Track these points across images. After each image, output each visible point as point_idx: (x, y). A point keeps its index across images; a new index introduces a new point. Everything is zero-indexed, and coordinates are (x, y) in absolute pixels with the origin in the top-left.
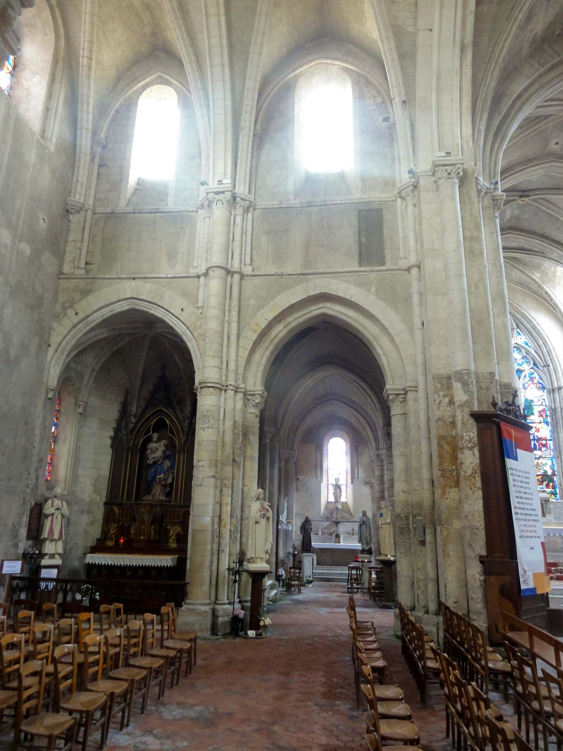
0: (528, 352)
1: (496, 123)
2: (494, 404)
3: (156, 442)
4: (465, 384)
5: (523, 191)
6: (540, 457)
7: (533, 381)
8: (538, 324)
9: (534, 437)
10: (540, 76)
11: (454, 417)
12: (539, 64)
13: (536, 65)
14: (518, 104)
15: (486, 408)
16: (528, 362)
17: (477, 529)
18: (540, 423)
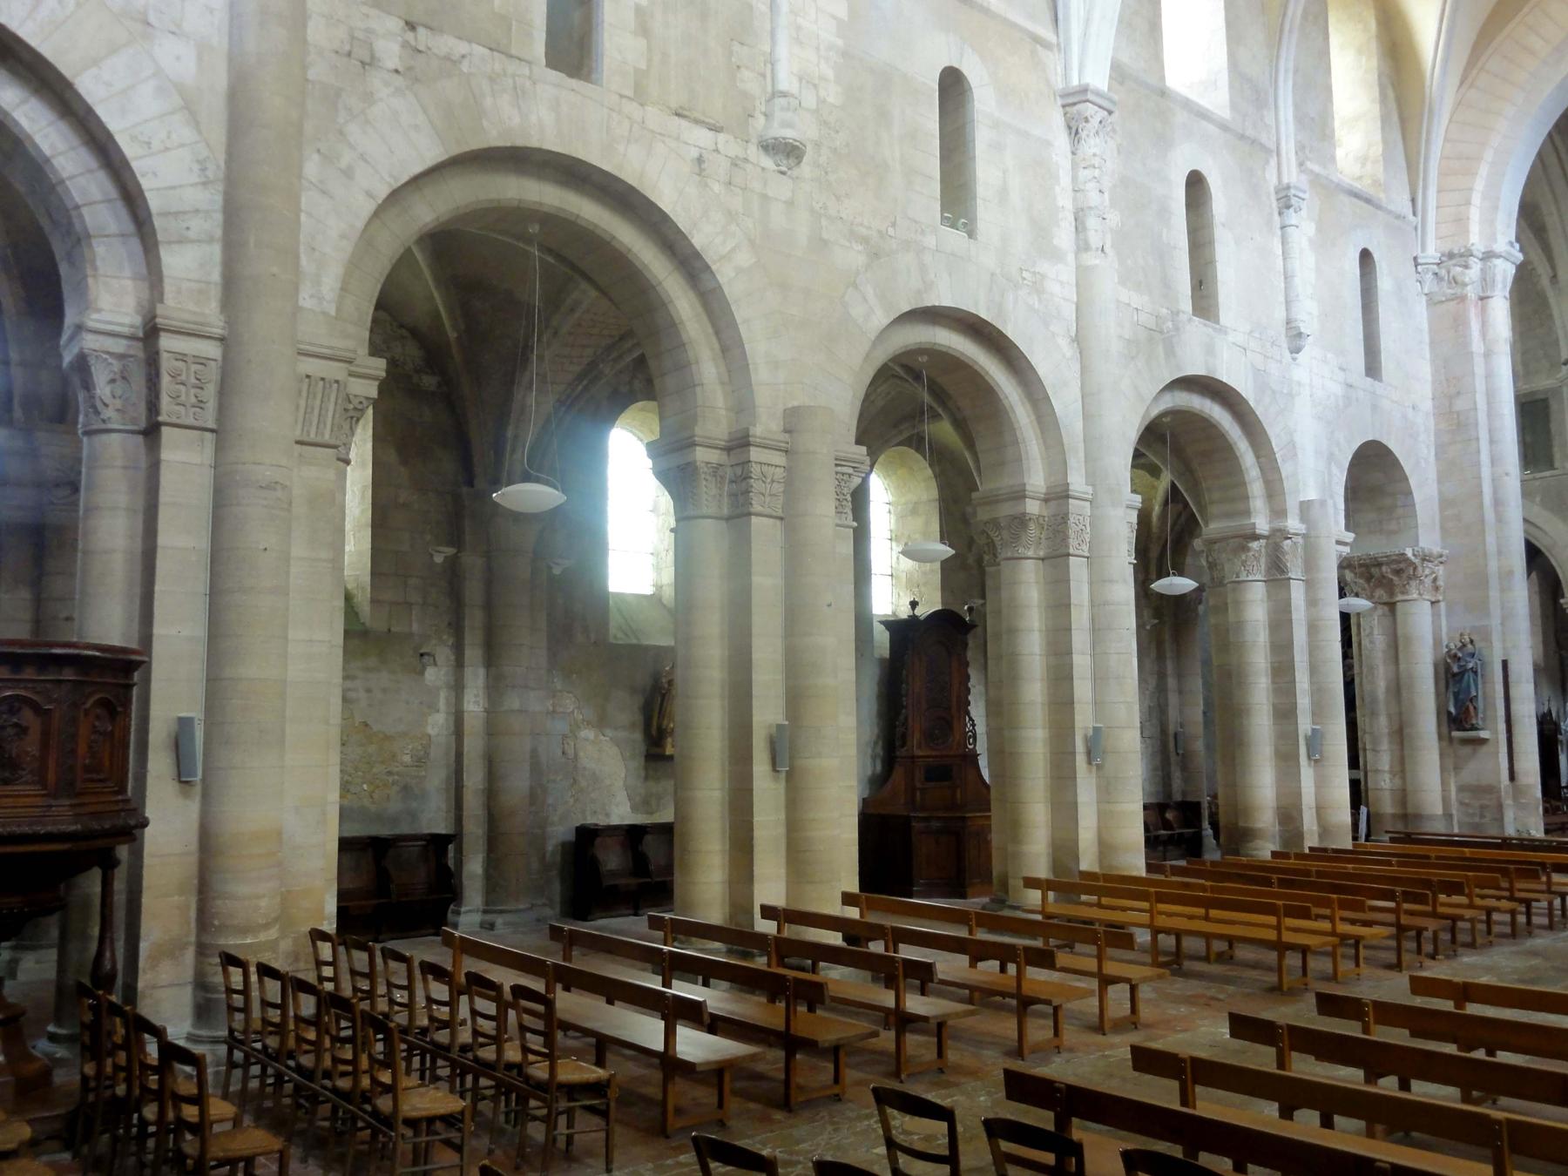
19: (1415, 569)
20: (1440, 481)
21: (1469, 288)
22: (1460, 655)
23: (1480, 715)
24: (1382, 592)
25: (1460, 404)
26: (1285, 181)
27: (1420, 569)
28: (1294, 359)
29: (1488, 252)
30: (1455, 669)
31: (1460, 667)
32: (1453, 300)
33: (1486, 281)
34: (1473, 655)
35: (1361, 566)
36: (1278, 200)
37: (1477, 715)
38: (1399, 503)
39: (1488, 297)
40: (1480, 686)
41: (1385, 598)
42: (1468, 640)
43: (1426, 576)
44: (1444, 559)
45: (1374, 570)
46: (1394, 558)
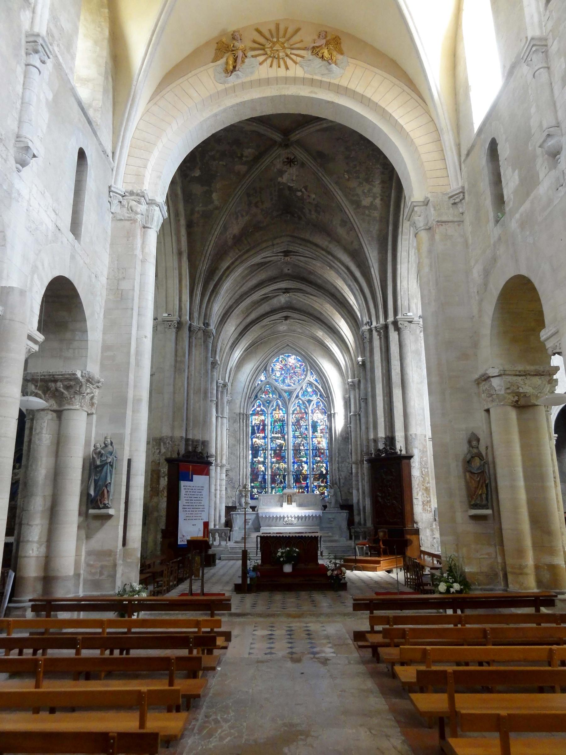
0: (316, 387)
1: (211, 287)
2: (178, 454)
3: (18, 469)
4: (165, 444)
5: (286, 289)
6: (319, 462)
7: (318, 408)
8: (323, 367)
9: (316, 447)
10: (240, 256)
11: (160, 460)
12: (239, 250)
13: (237, 251)
14: (228, 272)
15: (175, 456)
16: (317, 394)
17: (162, 516)
18: (321, 437)
19: (81, 387)
20: (104, 333)
21: (139, 216)
22: (103, 452)
23: (111, 498)
24: (54, 402)
25: (124, 285)
26: (36, 30)
27: (84, 387)
28: (19, 171)
29: (152, 200)
30: (98, 463)
31: (101, 461)
32: (128, 220)
33: (148, 216)
34: (111, 453)
35: (42, 380)
36: (27, 42)
37: (108, 496)
38: (77, 338)
39: (148, 228)
40: (113, 477)
41: (55, 407)
42: (110, 442)
43: (87, 394)
44: (100, 384)
45: (52, 385)
46: (67, 376)
